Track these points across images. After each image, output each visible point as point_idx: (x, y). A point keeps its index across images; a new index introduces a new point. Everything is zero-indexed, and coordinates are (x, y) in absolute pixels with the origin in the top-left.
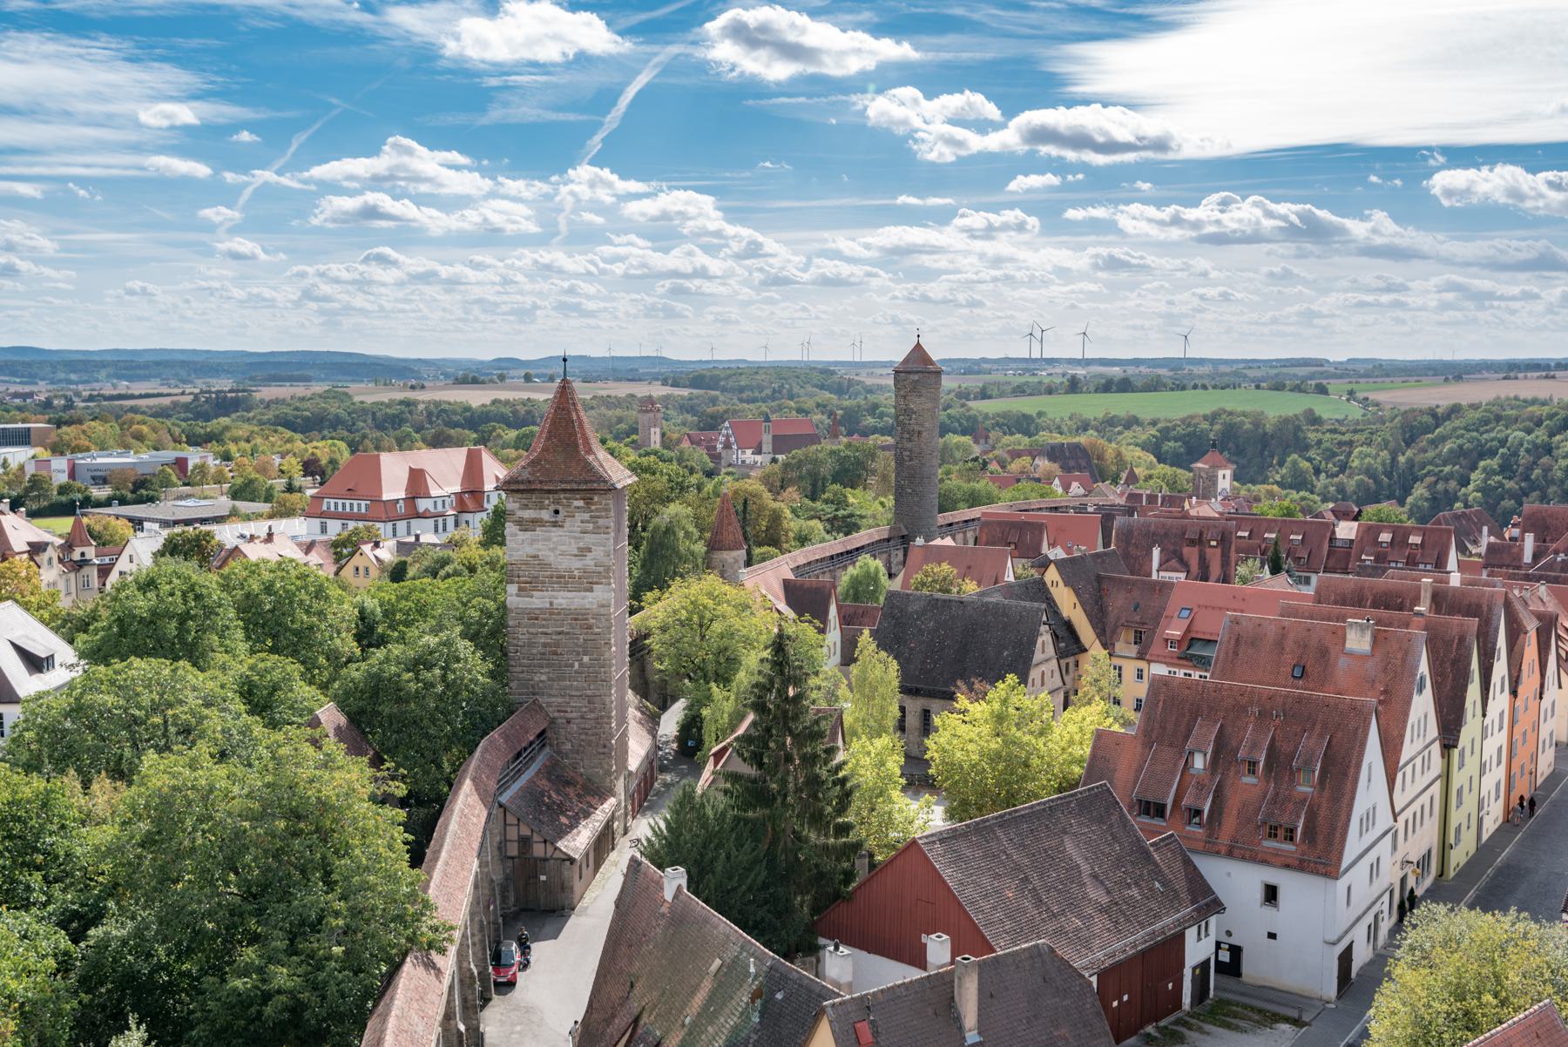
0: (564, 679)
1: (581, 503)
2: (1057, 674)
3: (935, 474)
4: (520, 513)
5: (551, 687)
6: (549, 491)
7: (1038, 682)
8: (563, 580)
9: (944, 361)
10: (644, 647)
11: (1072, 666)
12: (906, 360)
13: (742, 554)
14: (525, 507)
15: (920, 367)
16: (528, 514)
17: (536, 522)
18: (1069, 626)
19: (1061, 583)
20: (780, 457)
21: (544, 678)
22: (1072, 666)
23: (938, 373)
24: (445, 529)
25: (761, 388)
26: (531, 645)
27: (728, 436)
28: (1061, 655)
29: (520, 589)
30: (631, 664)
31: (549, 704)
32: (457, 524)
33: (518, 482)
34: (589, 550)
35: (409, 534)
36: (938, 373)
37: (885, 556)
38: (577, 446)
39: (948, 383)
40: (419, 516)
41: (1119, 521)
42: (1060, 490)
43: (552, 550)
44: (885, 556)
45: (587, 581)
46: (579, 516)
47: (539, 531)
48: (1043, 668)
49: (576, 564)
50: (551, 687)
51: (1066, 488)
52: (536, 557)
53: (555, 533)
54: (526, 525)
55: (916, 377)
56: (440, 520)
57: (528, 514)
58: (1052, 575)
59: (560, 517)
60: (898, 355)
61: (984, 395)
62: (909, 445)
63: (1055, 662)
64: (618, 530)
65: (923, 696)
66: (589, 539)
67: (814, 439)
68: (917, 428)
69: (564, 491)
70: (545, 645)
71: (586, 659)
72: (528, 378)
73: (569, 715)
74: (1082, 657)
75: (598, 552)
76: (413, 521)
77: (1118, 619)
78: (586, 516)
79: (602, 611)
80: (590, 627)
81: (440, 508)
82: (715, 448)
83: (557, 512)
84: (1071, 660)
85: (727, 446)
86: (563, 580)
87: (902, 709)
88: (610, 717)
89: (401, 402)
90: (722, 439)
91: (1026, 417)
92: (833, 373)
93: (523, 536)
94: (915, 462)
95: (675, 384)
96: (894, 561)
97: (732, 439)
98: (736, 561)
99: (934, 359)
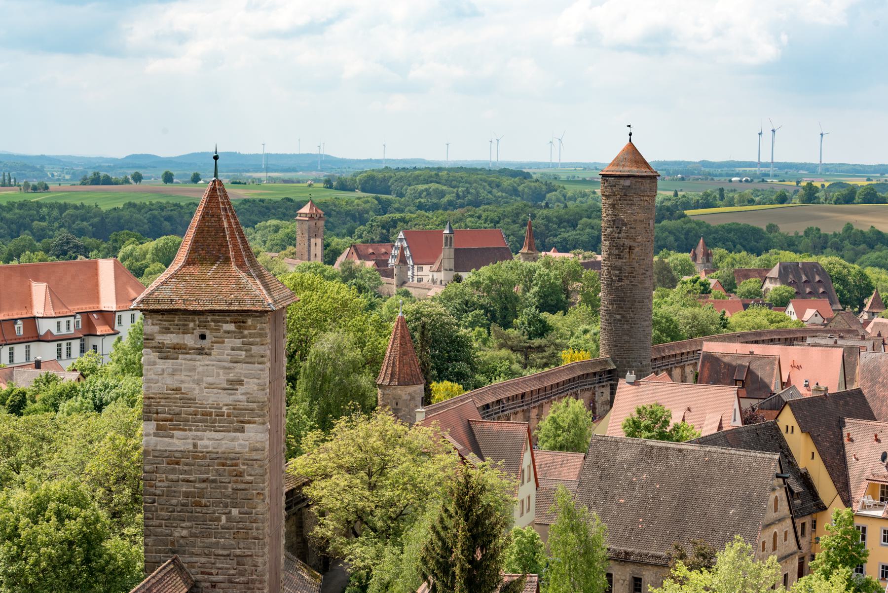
0: (209, 536)
1: (231, 327)
2: (791, 536)
3: (650, 298)
4: (159, 338)
5: (194, 545)
6: (195, 312)
7: (769, 545)
8: (210, 418)
9: (659, 163)
10: (304, 499)
11: (808, 527)
12: (617, 162)
13: (418, 389)
14: (166, 330)
15: (635, 171)
16: (170, 339)
17: (178, 349)
18: (805, 479)
19: (797, 429)
20: (465, 275)
21: (185, 533)
22: (808, 527)
23: (653, 178)
24: (69, 355)
25: (442, 194)
26: (170, 494)
27: (402, 249)
28: (795, 513)
29: (159, 428)
30: (288, 518)
31: (192, 565)
32: (83, 350)
33: (158, 301)
34: (241, 382)
35: (28, 359)
36: (653, 178)
37: (588, 394)
38: (227, 260)
39: (663, 194)
40: (39, 339)
41: (865, 357)
42: (794, 318)
43: (198, 382)
44: (588, 394)
45: (237, 420)
46: (230, 342)
47: (182, 360)
48: (775, 529)
49: (225, 399)
50: (194, 545)
51: (800, 314)
52: (178, 389)
53: (201, 362)
54: (166, 352)
55: (627, 183)
56: (64, 343)
57: (170, 339)
58: (787, 419)
59: (206, 343)
60: (604, 153)
61: (707, 203)
62: (619, 263)
63: (789, 522)
64: (276, 359)
65: (634, 563)
66: (241, 369)
67: (504, 254)
68: (628, 243)
69: (213, 312)
70: (187, 495)
71: (235, 512)
72: (168, 178)
73: (214, 578)
74: (819, 516)
75: (251, 386)
76: (32, 345)
77: (863, 471)
78: (238, 342)
79: (255, 456)
80: (240, 474)
81: (64, 330)
82: (386, 263)
83: (203, 337)
84: (808, 520)
85: (403, 260)
86: (210, 418)
87: (609, 576)
88: (261, 582)
89: (22, 205)
90: (395, 252)
91: (756, 232)
92: (527, 176)
93: (162, 365)
94: (625, 283)
95: (343, 186)
96: (599, 400)
97: (407, 253)
98: (413, 398)
99: (648, 160)
